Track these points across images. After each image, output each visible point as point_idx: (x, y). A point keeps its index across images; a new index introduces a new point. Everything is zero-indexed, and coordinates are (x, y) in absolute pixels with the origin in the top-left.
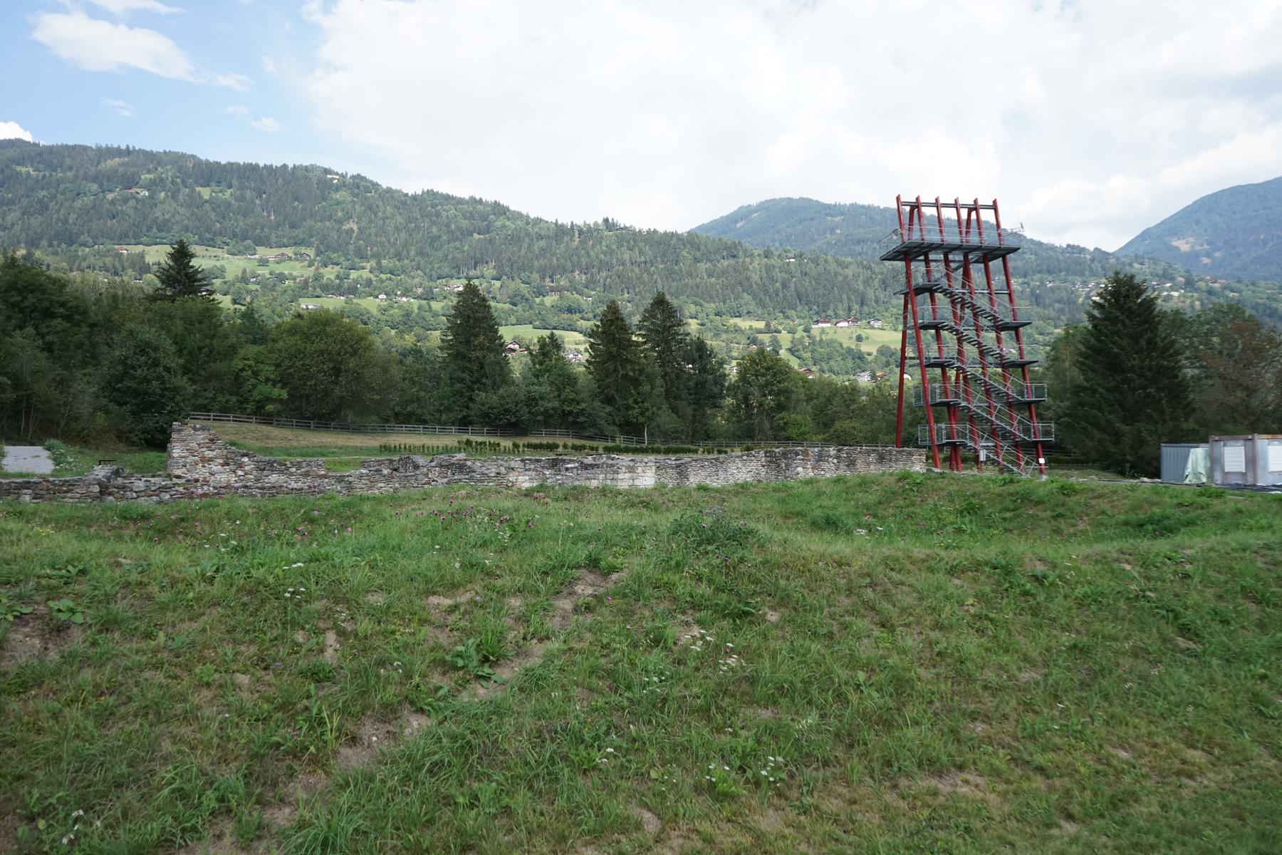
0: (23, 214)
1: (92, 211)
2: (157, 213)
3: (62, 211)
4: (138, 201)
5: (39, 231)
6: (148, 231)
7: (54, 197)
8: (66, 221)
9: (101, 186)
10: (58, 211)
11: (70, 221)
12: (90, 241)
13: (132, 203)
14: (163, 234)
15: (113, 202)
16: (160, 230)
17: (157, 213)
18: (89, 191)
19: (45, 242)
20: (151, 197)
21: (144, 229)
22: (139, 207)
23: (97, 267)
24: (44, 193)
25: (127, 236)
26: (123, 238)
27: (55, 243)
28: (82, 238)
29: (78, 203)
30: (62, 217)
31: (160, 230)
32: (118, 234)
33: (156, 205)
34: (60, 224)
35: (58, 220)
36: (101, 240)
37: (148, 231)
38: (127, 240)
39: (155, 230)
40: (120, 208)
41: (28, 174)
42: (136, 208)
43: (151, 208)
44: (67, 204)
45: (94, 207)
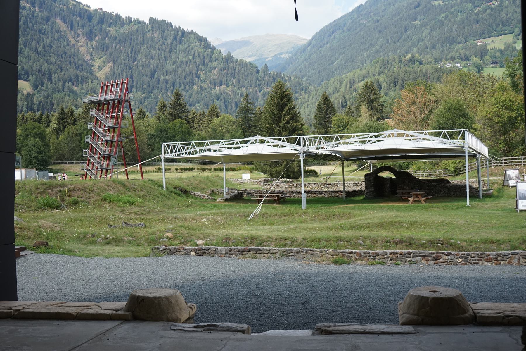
0: (432, 30)
1: (465, 22)
2: (503, 15)
3: (449, 25)
4: (492, 9)
5: (436, 39)
6: (497, 27)
7: (447, 16)
8: (451, 31)
9: (473, 4)
10: (448, 25)
11: (454, 30)
12: (463, 39)
13: (488, 11)
14: (507, 28)
15: (477, 14)
16: (504, 26)
17: (503, 15)
18: (467, 9)
19: (439, 46)
20: (500, 5)
21: (494, 27)
22: (493, 13)
23: (456, 57)
24: (443, 15)
25: (484, 33)
26: (481, 35)
27: (444, 44)
28: (459, 39)
29: (458, 19)
30: (449, 28)
31: (504, 26)
32: (478, 33)
33: (502, 10)
34: (448, 33)
35: (448, 30)
36: (470, 38)
37: (497, 27)
38: (483, 35)
39: (501, 26)
40: (481, 16)
41: (439, 5)
42: (491, 15)
43: (500, 12)
44: (452, 20)
45: (467, 19)
